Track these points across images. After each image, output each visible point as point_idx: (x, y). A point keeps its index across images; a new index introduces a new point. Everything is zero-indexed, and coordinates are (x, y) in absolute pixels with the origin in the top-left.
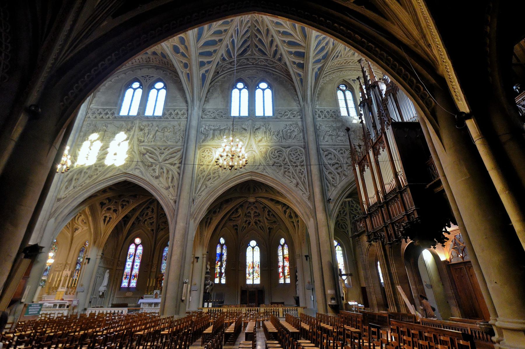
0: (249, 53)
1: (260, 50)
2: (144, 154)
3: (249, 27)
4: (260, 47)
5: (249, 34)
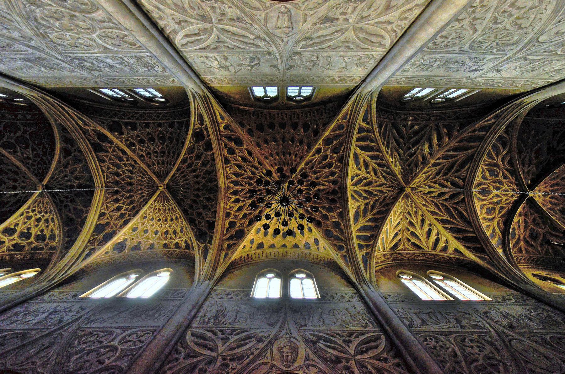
0: (401, 247)
1: (414, 244)
3: (401, 219)
4: (413, 240)
5: (400, 227)
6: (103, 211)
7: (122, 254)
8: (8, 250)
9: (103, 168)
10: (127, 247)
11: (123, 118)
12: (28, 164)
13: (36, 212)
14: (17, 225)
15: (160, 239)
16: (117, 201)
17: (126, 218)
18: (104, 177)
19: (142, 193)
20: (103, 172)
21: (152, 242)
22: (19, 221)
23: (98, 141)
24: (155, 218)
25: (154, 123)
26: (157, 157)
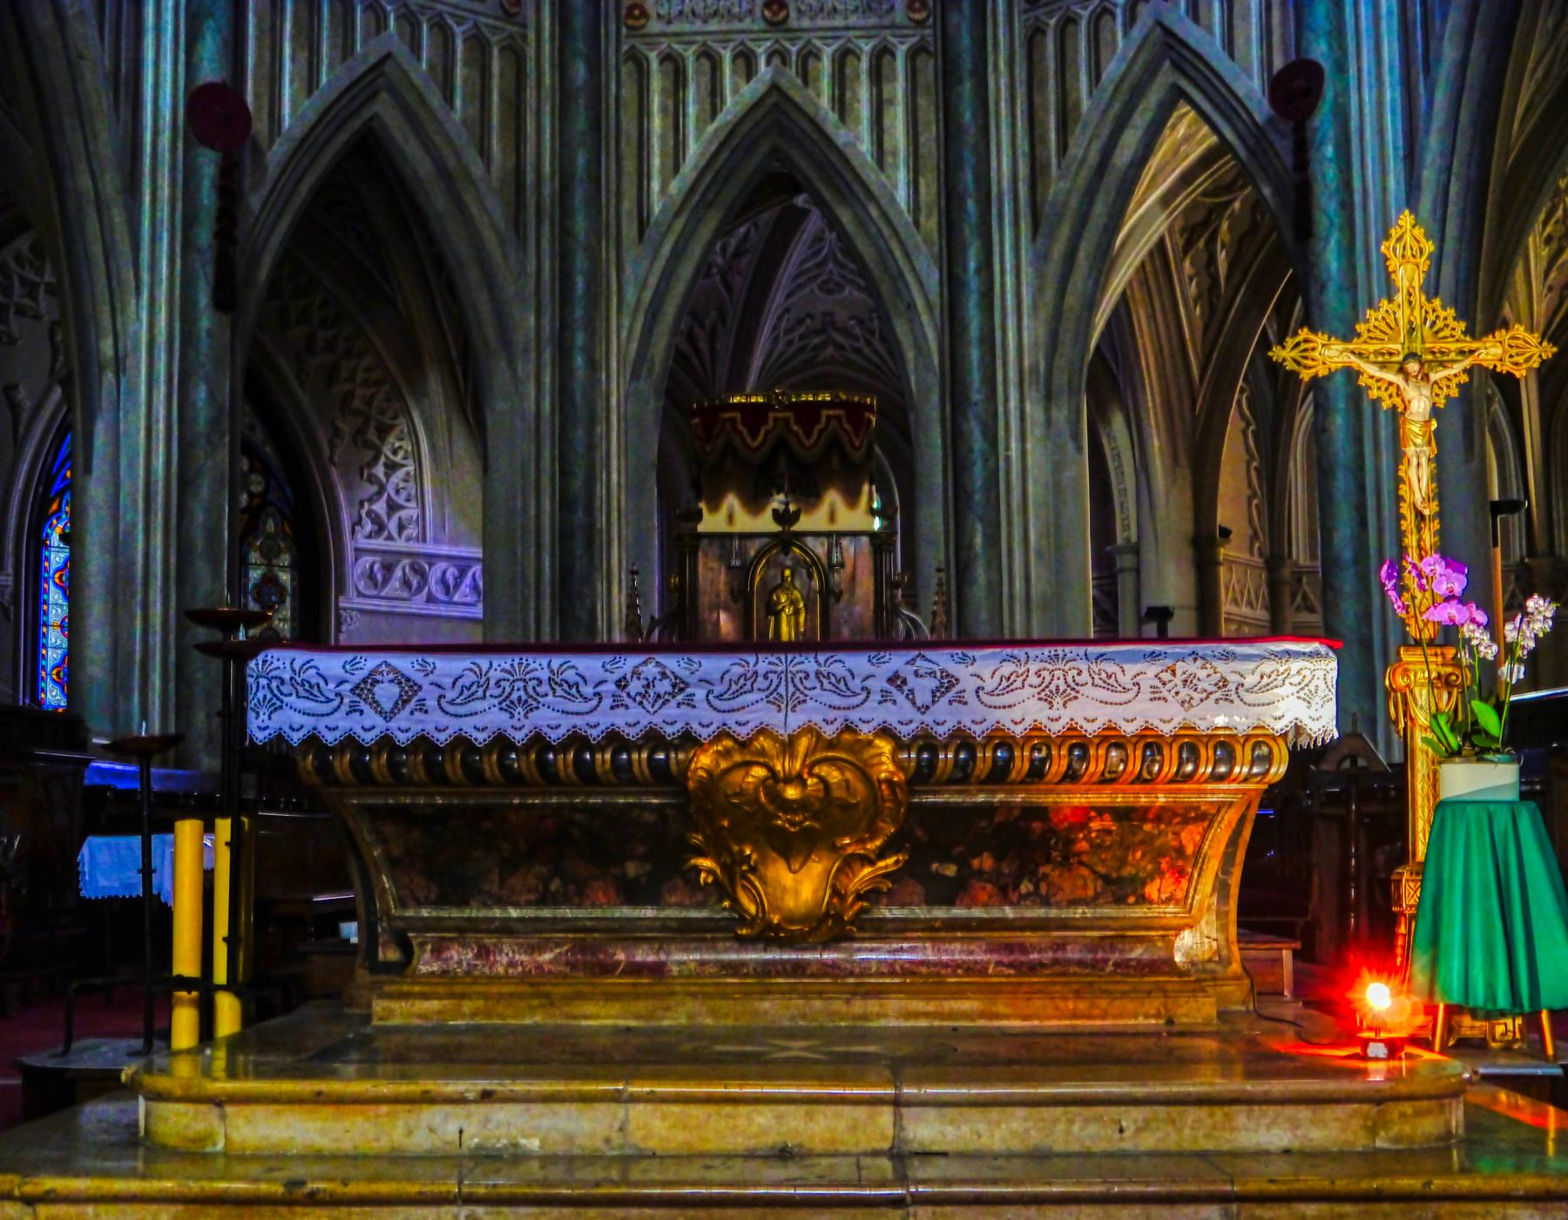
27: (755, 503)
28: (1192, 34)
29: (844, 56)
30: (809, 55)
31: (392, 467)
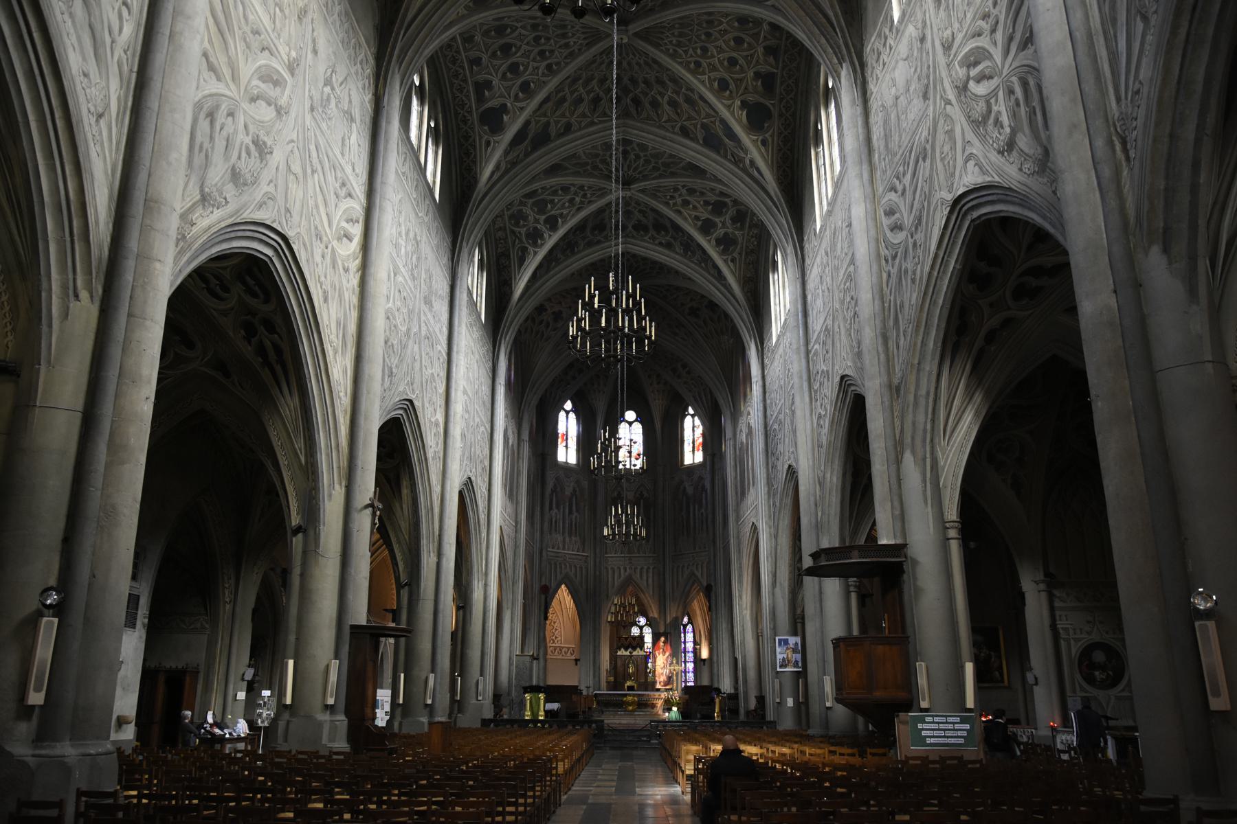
2: (965, 88)
6: (677, 129)
7: (775, 113)
8: (742, 228)
9: (583, 124)
10: (762, 100)
11: (470, 107)
12: (582, 202)
13: (676, 195)
14: (697, 218)
15: (756, 36)
16: (655, 104)
17: (696, 97)
18: (601, 122)
19: (638, 64)
20: (592, 124)
21: (760, 50)
22: (690, 216)
23: (526, 142)
24: (702, 44)
25: (466, 50)
26: (548, 39)
27: (626, 650)
28: (696, 572)
29: (642, 569)
30: (636, 568)
31: (556, 630)
